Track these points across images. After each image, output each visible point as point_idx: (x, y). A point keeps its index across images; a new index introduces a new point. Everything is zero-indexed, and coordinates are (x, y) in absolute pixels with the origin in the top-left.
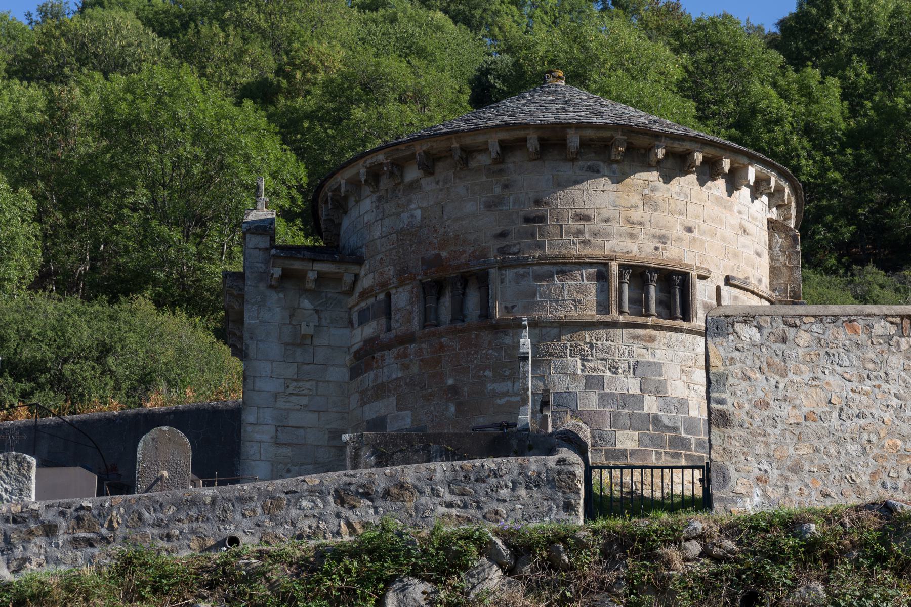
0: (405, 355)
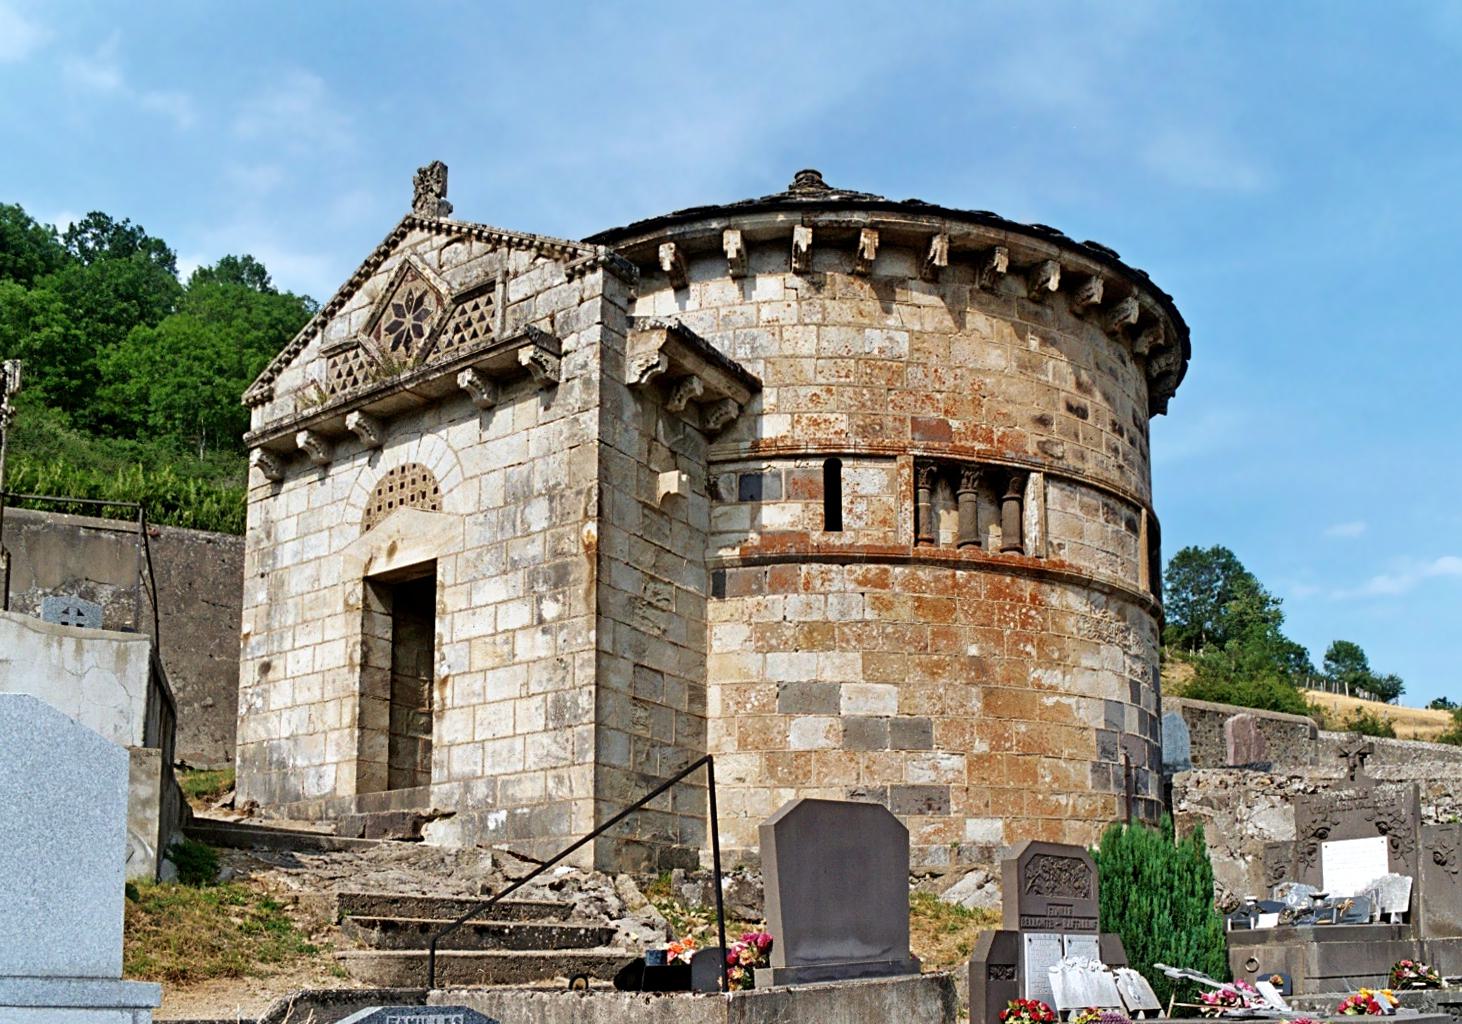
0: (882, 583)
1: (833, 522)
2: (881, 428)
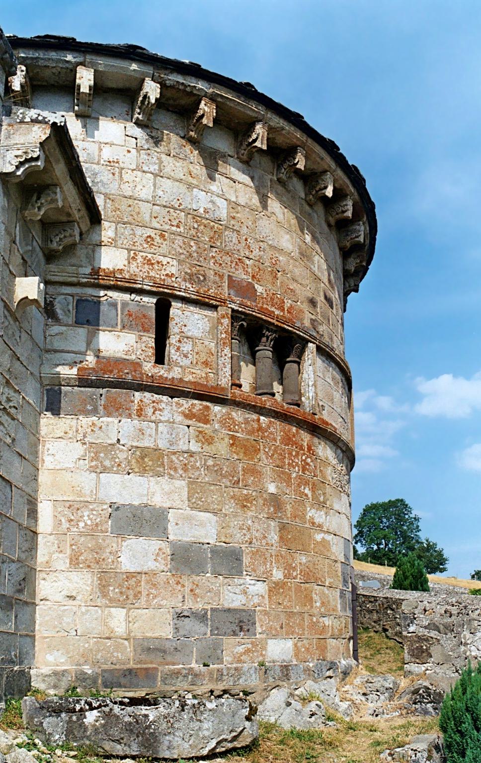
1: (160, 358)
2: (205, 279)
